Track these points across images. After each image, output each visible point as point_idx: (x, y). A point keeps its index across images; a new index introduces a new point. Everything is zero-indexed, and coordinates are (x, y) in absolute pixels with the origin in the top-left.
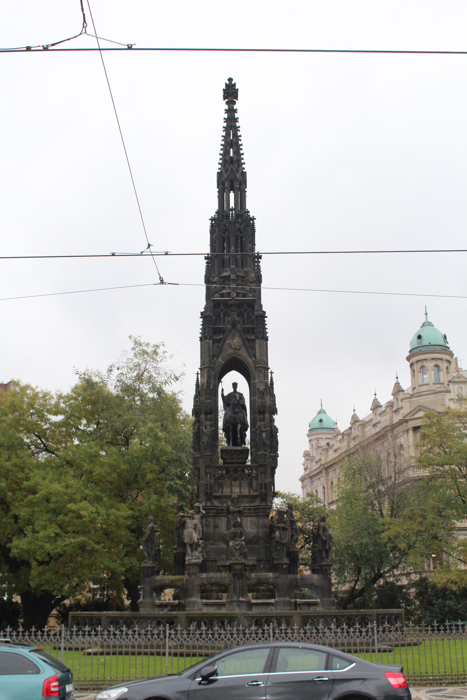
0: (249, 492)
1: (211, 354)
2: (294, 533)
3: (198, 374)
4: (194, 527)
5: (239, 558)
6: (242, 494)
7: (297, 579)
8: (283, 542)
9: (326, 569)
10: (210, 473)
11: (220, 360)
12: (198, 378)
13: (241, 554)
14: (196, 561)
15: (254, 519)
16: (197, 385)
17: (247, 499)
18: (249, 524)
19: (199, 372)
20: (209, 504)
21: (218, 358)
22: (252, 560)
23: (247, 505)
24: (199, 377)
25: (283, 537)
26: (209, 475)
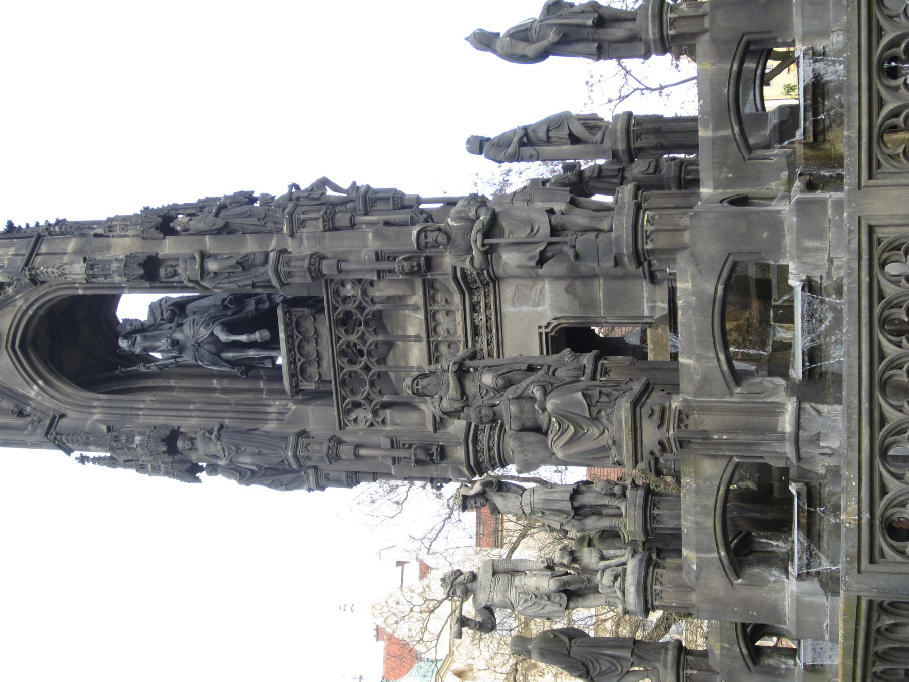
0: (416, 308)
1: (20, 422)
2: (565, 133)
3: (83, 460)
4: (503, 579)
5: (612, 430)
6: (424, 335)
7: (714, 141)
8: (545, 230)
9: (673, 22)
10: (358, 446)
11: (33, 392)
12: (96, 460)
13: (595, 419)
14: (631, 581)
15: (508, 291)
16: (112, 462)
17: (441, 317)
18: (525, 308)
19: (77, 454)
20: (459, 453)
21: (26, 399)
22: (652, 300)
23: (459, 316)
24: (91, 454)
25: (522, 234)
26: (362, 452)
